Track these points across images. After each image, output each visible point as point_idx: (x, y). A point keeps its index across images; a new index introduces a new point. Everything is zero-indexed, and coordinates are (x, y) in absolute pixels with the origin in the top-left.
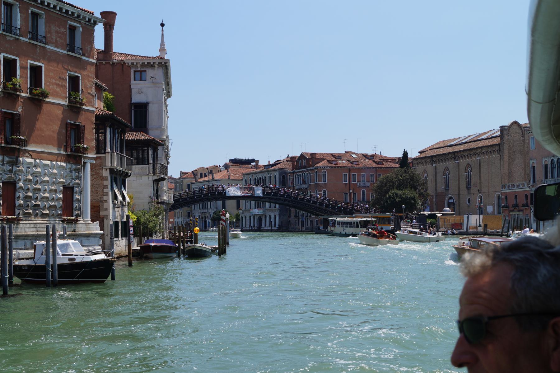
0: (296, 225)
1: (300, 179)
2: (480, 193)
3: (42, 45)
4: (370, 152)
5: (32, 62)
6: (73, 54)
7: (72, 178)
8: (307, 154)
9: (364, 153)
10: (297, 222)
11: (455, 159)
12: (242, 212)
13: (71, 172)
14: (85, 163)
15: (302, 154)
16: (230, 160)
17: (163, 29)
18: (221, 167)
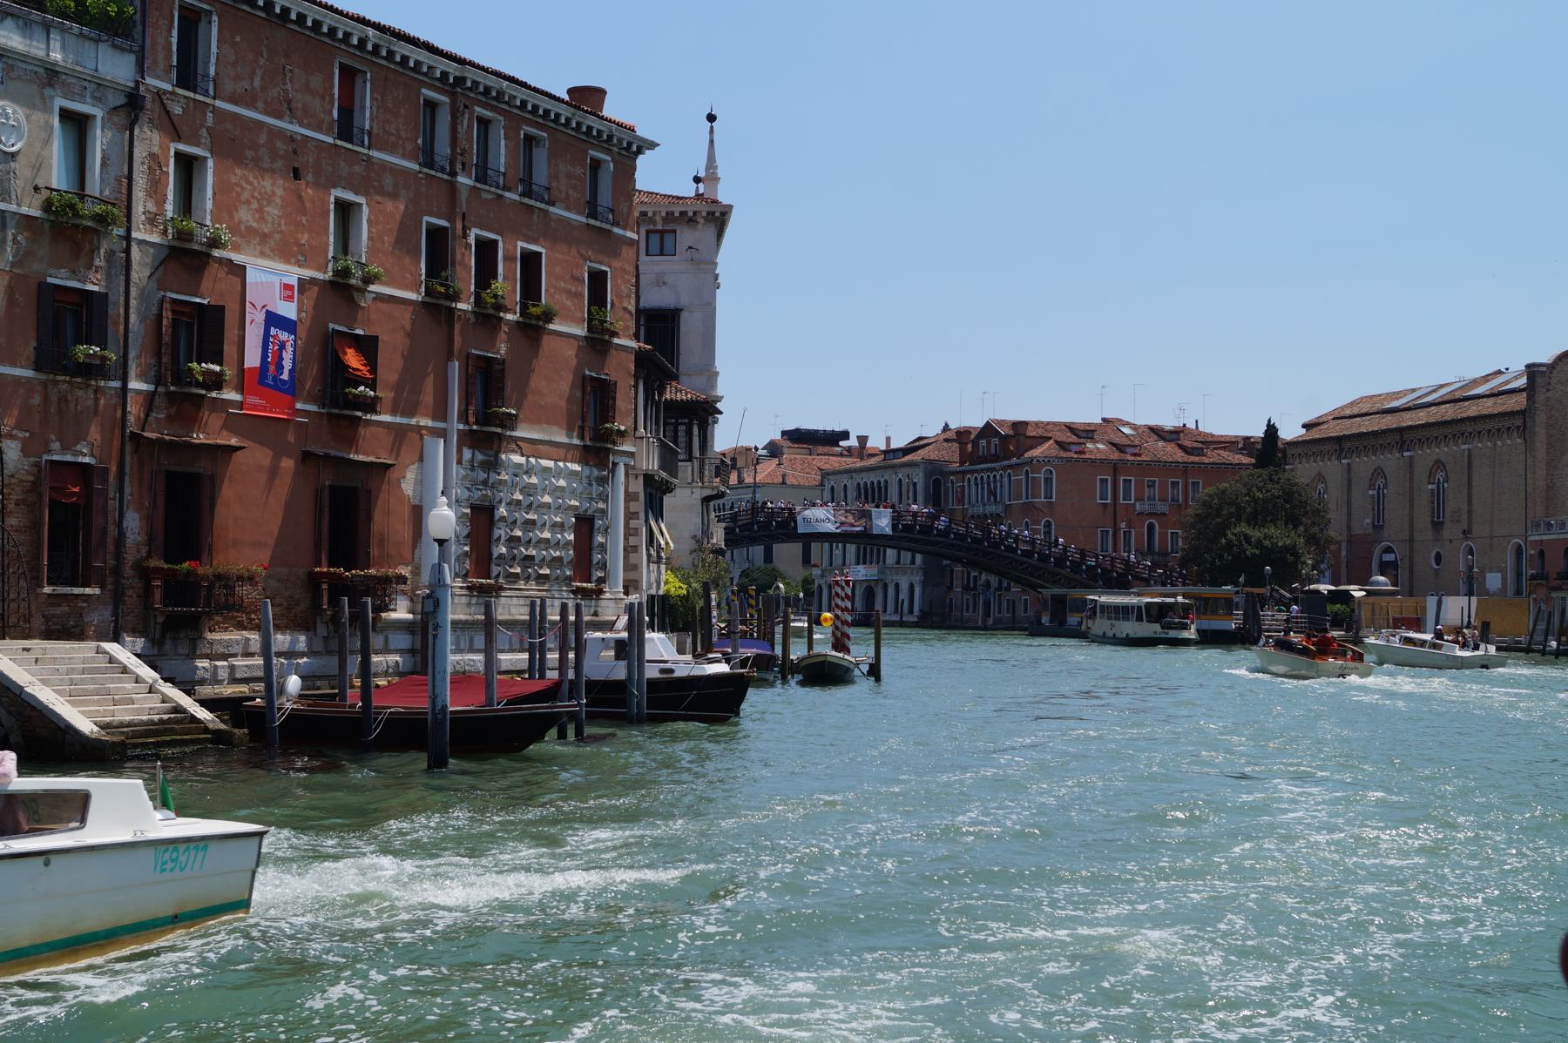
0: (967, 612)
1: (983, 488)
2: (1467, 539)
3: (543, 206)
4: (1169, 422)
5: (525, 245)
6: (598, 224)
7: (591, 499)
8: (1001, 423)
9: (1152, 423)
10: (971, 602)
11: (1402, 446)
12: (819, 572)
13: (590, 484)
14: (615, 464)
15: (988, 424)
16: (784, 433)
17: (712, 127)
18: (761, 452)
